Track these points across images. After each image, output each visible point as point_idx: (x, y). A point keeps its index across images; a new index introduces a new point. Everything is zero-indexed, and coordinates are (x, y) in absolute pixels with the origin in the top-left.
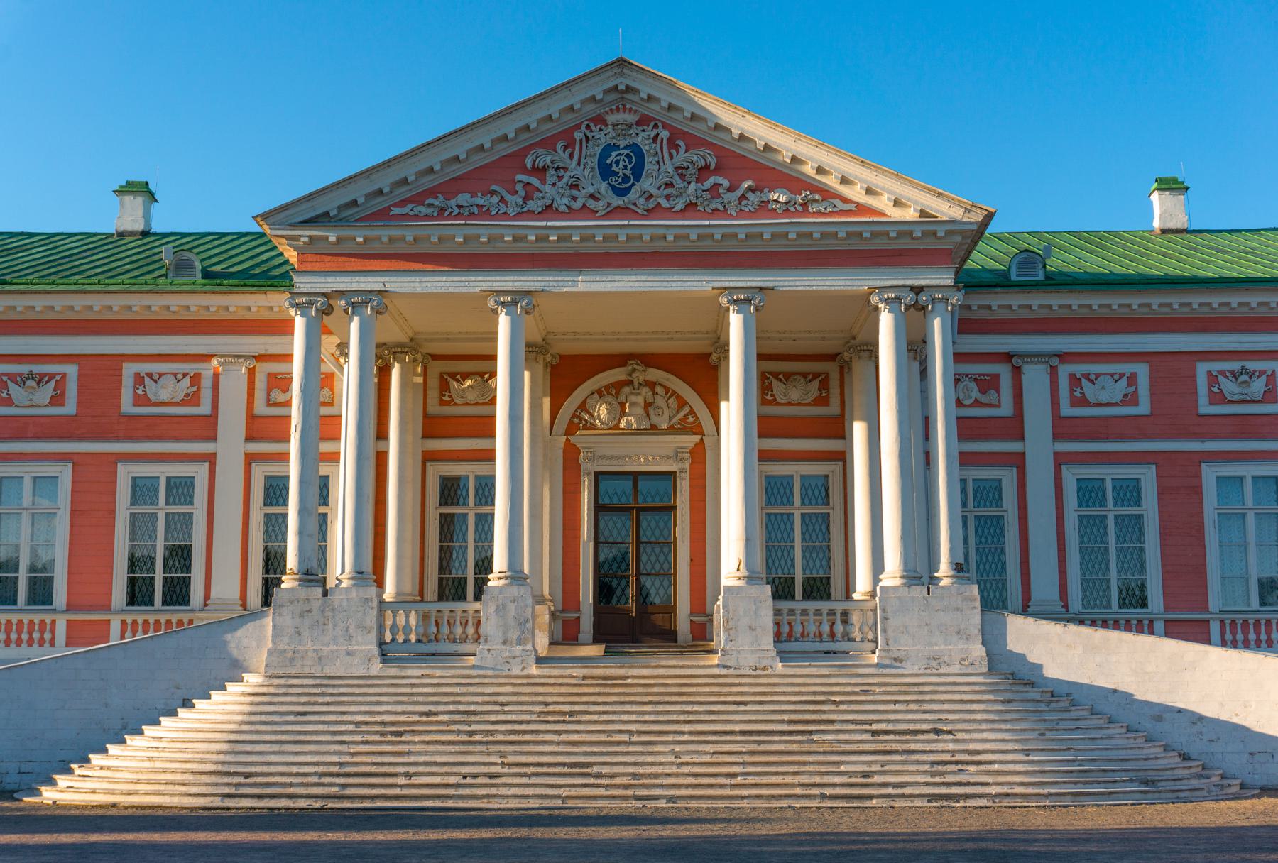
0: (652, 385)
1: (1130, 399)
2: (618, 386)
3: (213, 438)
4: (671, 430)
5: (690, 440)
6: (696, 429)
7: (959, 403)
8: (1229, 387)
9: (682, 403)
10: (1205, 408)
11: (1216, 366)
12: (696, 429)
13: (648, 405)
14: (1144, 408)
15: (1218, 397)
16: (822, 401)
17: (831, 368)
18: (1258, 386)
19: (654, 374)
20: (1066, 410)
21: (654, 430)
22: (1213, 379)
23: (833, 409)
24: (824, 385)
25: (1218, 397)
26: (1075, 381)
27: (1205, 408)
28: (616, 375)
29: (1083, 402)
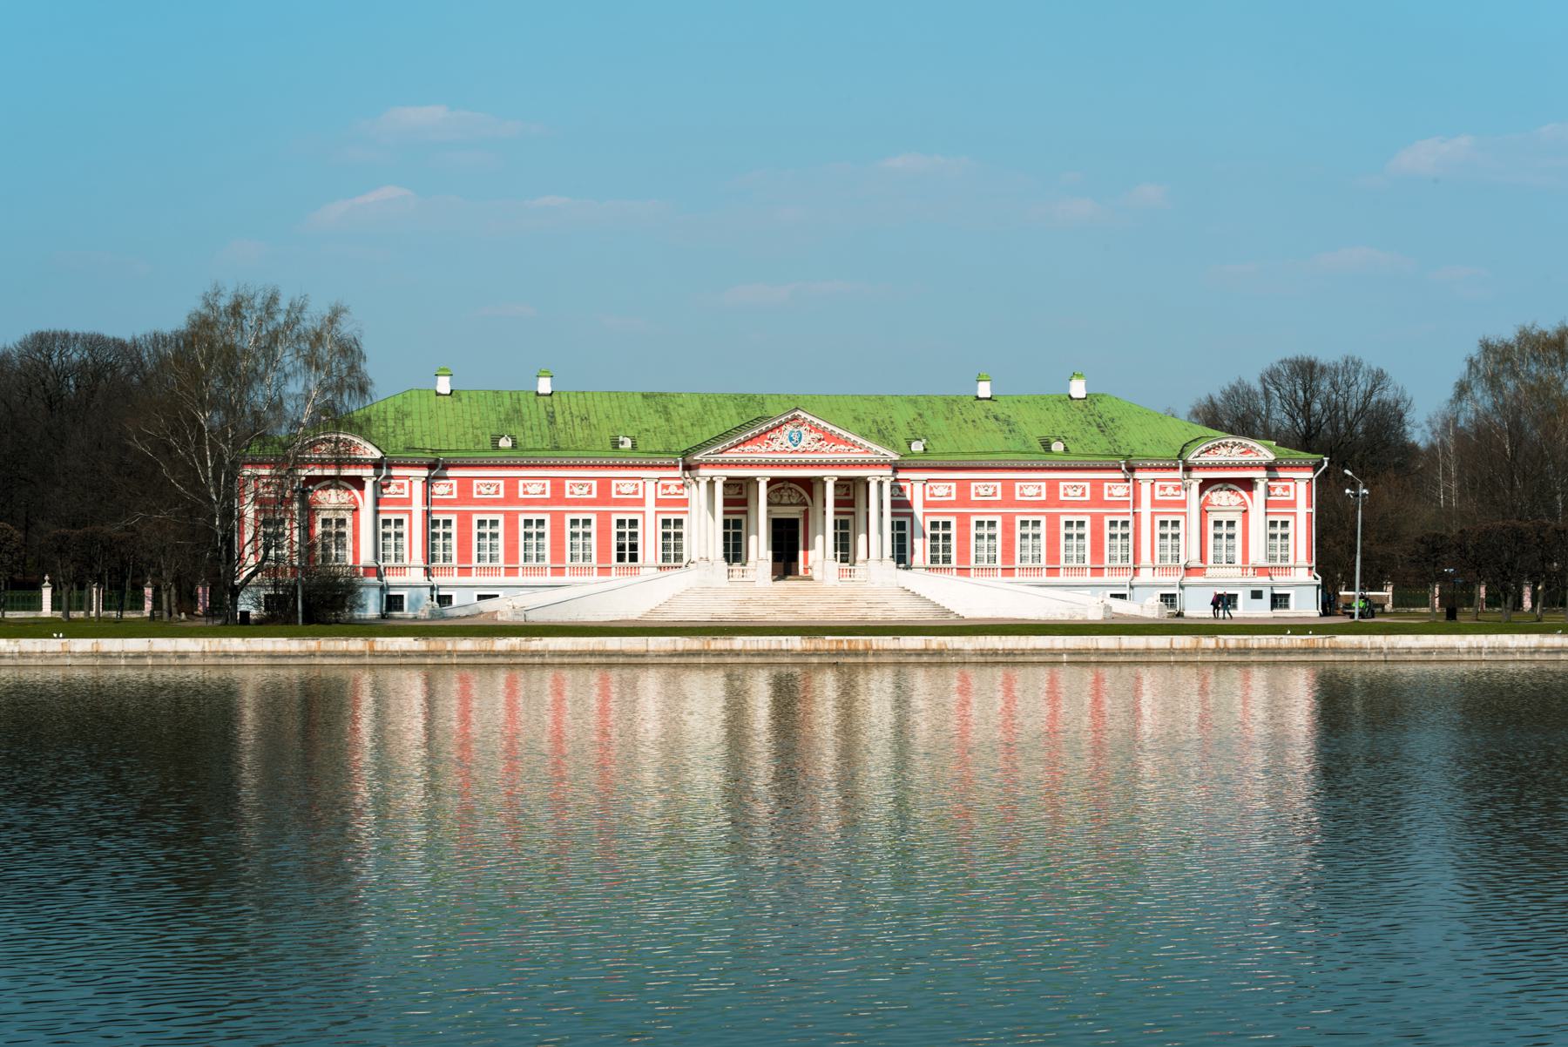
0: (791, 489)
1: (949, 495)
2: (780, 489)
3: (643, 505)
4: (797, 505)
5: (804, 508)
6: (806, 504)
7: (892, 495)
8: (982, 491)
9: (801, 495)
10: (973, 498)
11: (978, 484)
12: (806, 504)
13: (789, 496)
14: (953, 498)
15: (977, 494)
16: (847, 494)
17: (851, 483)
18: (991, 491)
19: (792, 485)
20: (928, 498)
21: (791, 504)
22: (976, 488)
23: (851, 497)
24: (848, 489)
25: (977, 494)
26: (931, 488)
27: (973, 498)
28: (780, 485)
29: (932, 495)
